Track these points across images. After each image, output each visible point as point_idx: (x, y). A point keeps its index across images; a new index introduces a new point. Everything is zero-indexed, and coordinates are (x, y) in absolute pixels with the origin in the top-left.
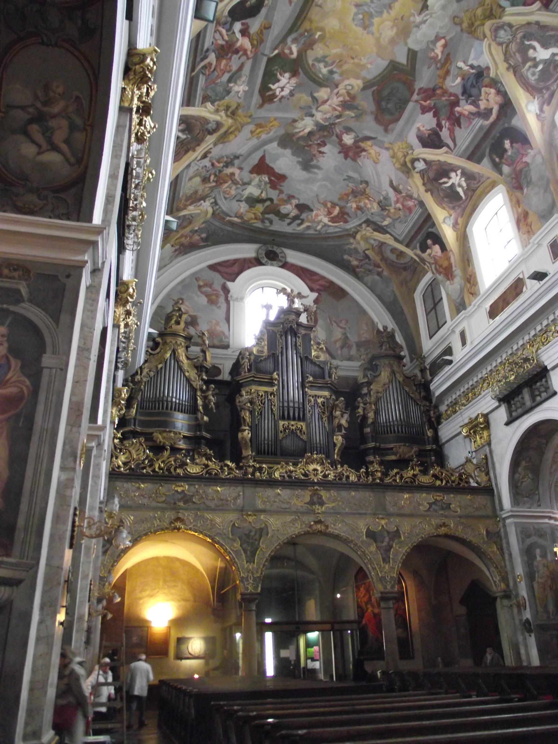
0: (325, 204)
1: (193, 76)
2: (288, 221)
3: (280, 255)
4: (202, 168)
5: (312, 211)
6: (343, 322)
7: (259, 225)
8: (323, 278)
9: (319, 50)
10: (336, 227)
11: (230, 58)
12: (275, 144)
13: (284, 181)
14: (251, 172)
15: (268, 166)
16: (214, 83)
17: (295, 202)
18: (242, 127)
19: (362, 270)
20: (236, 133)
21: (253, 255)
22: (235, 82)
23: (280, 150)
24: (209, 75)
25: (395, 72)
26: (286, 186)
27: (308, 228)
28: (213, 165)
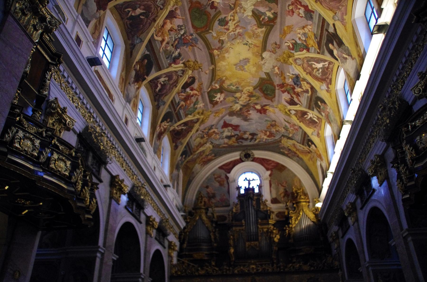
0: (262, 132)
1: (177, 113)
2: (249, 141)
3: (251, 155)
4: (198, 135)
5: (257, 135)
6: (284, 183)
7: (236, 144)
8: (273, 162)
9: (227, 83)
10: (271, 139)
11: (191, 99)
12: (227, 116)
13: (239, 127)
14: (223, 127)
15: (229, 124)
16: (187, 109)
17: (248, 133)
18: (209, 116)
19: (291, 155)
20: (207, 119)
21: (238, 158)
22: (197, 104)
23: (231, 118)
24: (184, 108)
25: (264, 81)
26: (240, 128)
27: (259, 141)
28: (203, 132)
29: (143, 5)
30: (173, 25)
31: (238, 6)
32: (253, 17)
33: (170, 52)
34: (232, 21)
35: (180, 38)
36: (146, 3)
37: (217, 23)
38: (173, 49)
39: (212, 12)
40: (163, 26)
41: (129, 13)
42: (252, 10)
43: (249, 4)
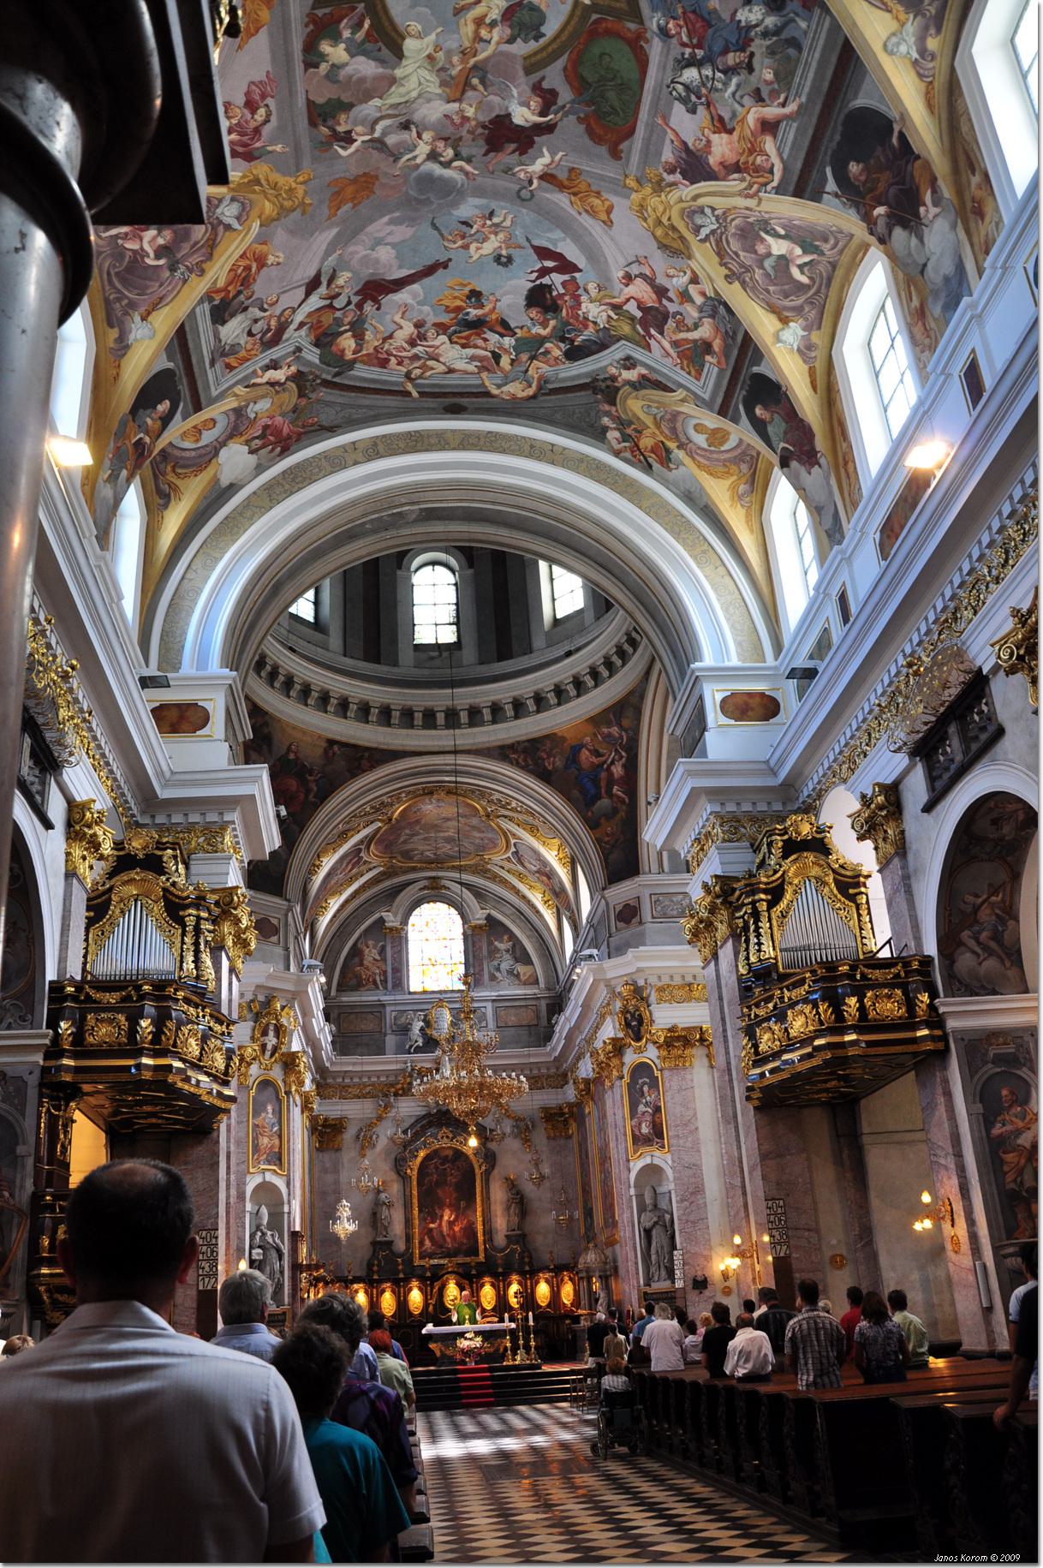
29: (755, 252)
30: (706, 131)
31: (452, 77)
32: (401, 28)
33: (771, 52)
34: (488, 21)
35: (708, 60)
36: (741, 253)
37: (551, 28)
38: (759, 46)
39: (554, 77)
40: (736, 168)
41: (806, 264)
42: (404, 62)
43: (412, 83)
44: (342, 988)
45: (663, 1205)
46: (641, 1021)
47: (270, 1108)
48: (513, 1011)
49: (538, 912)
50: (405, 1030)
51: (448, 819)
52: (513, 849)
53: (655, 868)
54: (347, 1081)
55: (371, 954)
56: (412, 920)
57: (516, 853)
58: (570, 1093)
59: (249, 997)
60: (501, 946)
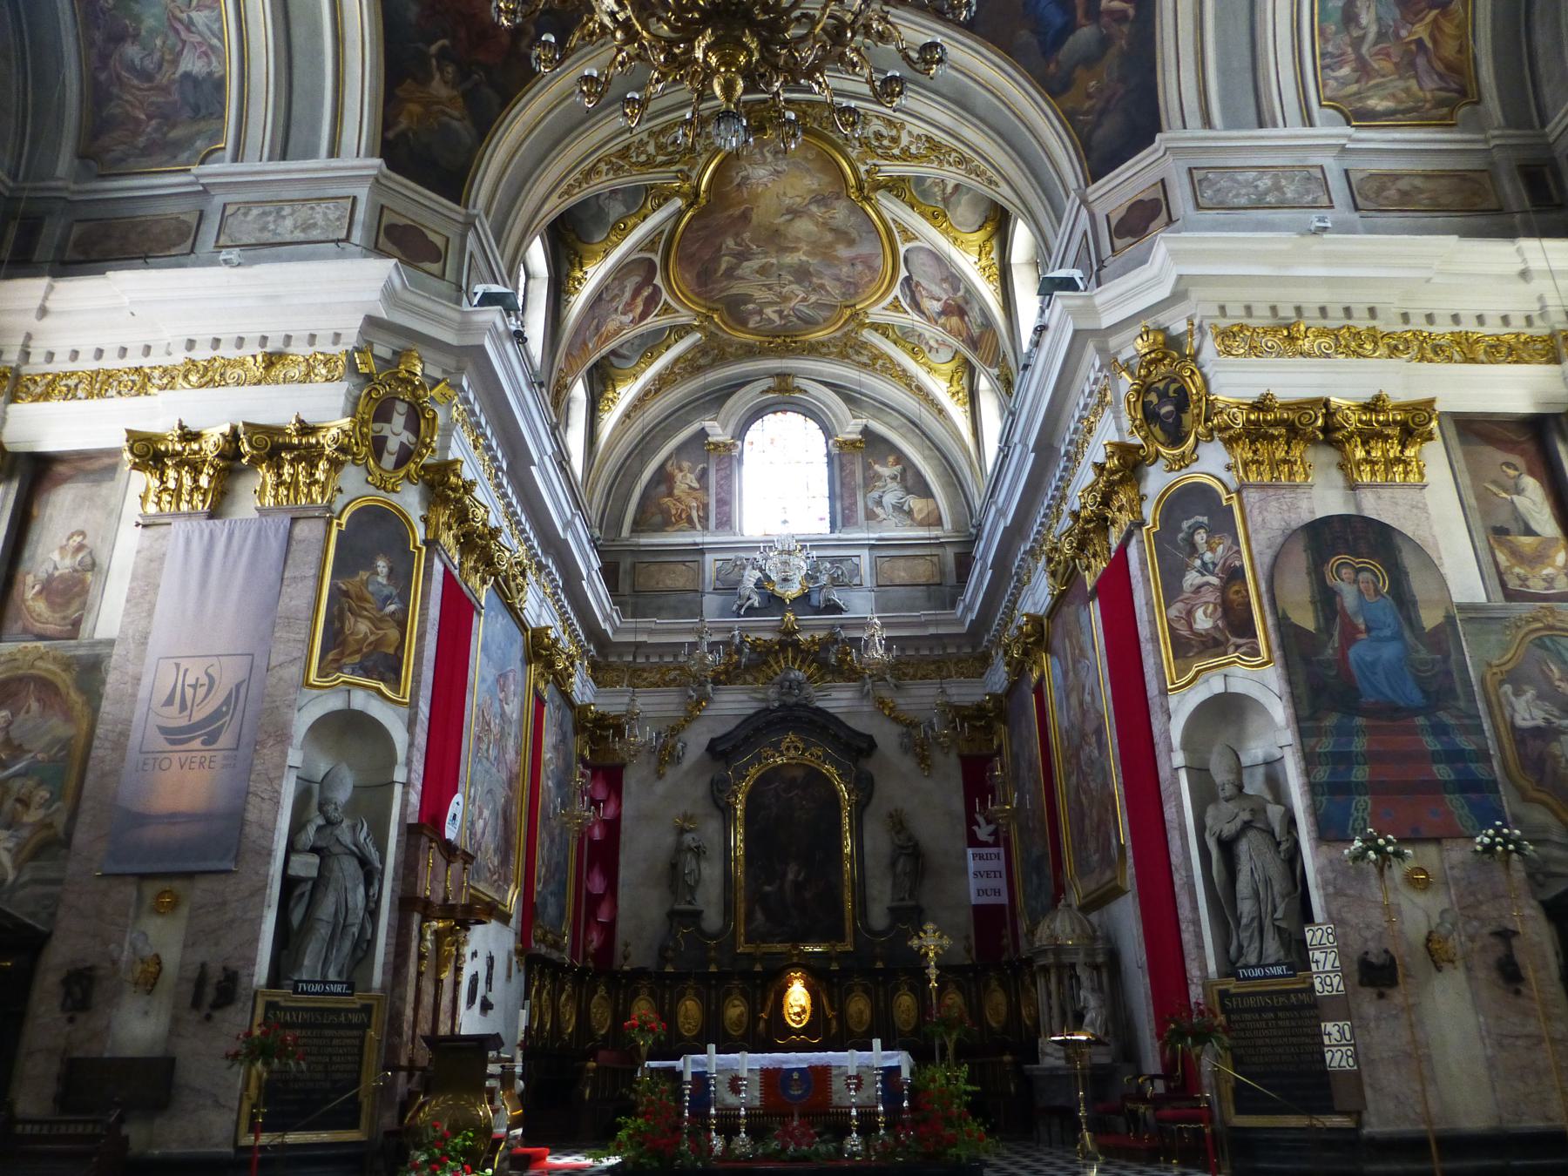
44: (639, 526)
45: (1255, 785)
46: (1182, 400)
47: (382, 565)
48: (901, 563)
49: (941, 411)
50: (729, 587)
51: (795, 213)
52: (903, 273)
53: (1194, 119)
54: (640, 660)
55: (685, 480)
56: (749, 436)
57: (908, 280)
58: (999, 677)
59: (351, 339)
60: (885, 471)
